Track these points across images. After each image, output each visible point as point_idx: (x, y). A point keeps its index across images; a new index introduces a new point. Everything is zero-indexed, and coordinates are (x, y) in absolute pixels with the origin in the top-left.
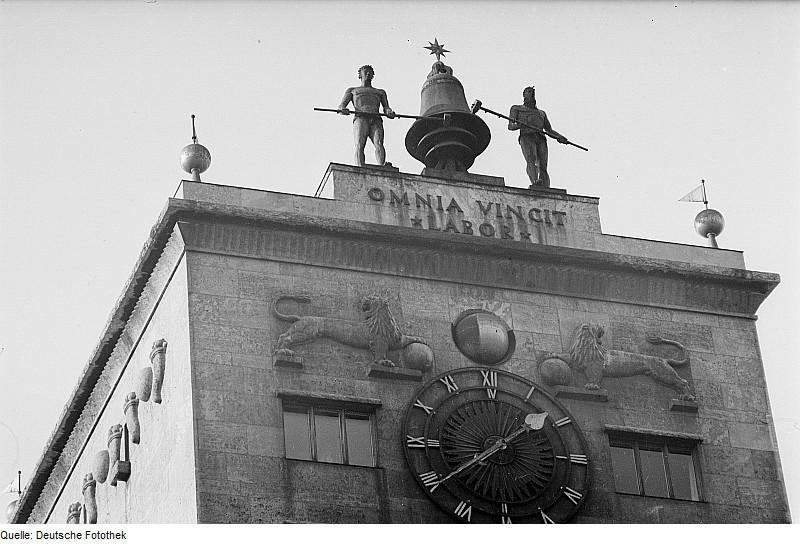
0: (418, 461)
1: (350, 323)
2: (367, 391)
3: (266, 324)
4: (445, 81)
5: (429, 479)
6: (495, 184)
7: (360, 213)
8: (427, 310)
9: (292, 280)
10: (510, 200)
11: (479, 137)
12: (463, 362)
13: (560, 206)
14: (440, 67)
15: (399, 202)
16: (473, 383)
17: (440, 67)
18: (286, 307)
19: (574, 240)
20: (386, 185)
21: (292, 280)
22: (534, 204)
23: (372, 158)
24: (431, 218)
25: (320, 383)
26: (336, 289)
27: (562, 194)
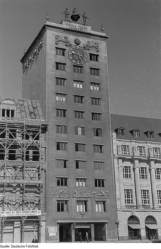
0: (70, 56)
1: (64, 39)
2: (65, 47)
8: (72, 38)
9: (58, 34)
10: (82, 26)
11: (79, 17)
12: (75, 45)
13: (87, 27)
15: (69, 25)
16: (76, 47)
20: (68, 23)
21: (58, 34)
22: (84, 26)
24: (73, 27)
25: (59, 46)
26: (62, 35)
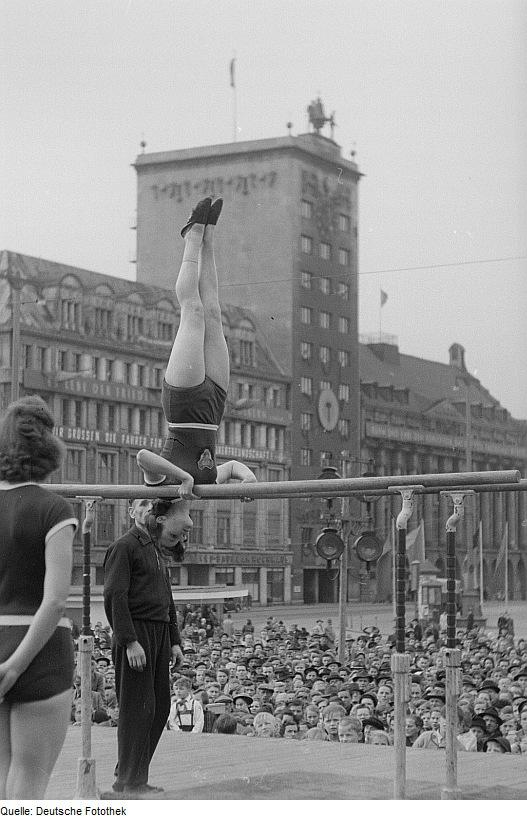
4: (319, 106)
7: (311, 148)
8: (321, 175)
18: (304, 174)
19: (339, 161)
21: (306, 167)
26: (309, 168)
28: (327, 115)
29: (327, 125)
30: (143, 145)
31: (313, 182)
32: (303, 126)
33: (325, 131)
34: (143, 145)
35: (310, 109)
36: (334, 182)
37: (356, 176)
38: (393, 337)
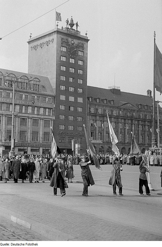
2: (66, 46)
3: (61, 40)
4: (72, 20)
5: (69, 53)
6: (74, 30)
7: (66, 32)
8: (70, 39)
9: (62, 37)
13: (78, 32)
14: (72, 18)
17: (72, 18)
18: (62, 39)
20: (68, 29)
21: (62, 37)
23: (67, 27)
25: (63, 45)
27: (78, 31)
28: (75, 22)
29: (75, 26)
30: (31, 37)
31: (66, 41)
32: (63, 25)
33: (74, 27)
34: (31, 37)
35: (67, 21)
36: (76, 42)
37: (88, 40)
38: (120, 87)
